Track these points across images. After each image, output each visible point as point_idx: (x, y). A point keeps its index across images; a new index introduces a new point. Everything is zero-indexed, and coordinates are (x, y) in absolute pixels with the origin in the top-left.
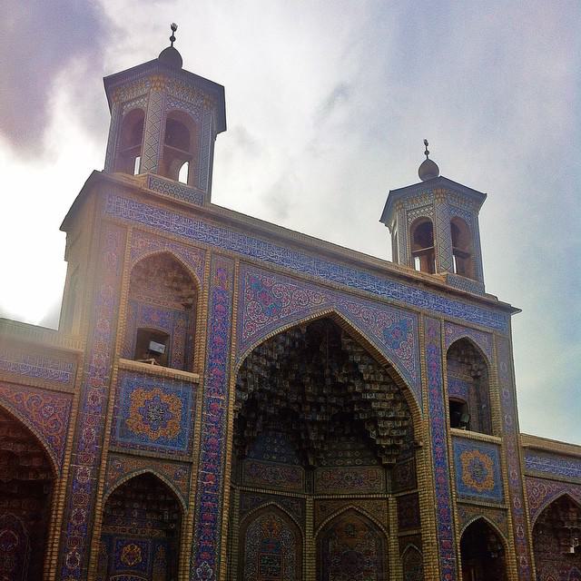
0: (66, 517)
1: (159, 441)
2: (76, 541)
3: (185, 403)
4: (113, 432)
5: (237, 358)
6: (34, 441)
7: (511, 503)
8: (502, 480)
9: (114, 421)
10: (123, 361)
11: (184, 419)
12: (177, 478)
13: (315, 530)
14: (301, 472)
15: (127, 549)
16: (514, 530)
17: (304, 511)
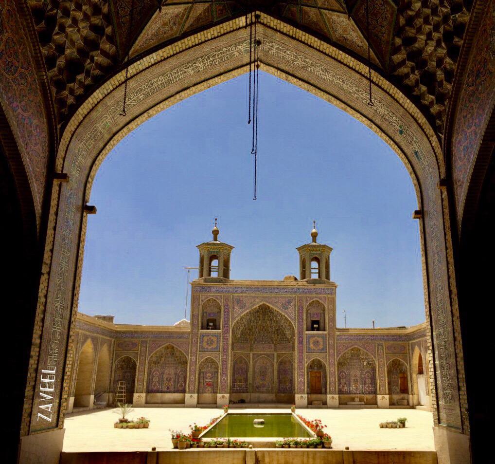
0: (190, 368)
1: (211, 349)
2: (192, 374)
3: (218, 338)
4: (200, 348)
5: (232, 324)
6: (182, 354)
7: (329, 352)
8: (326, 345)
9: (200, 346)
10: (201, 331)
11: (217, 341)
12: (216, 357)
13: (277, 362)
14: (273, 346)
15: (208, 374)
16: (329, 360)
17: (274, 356)
